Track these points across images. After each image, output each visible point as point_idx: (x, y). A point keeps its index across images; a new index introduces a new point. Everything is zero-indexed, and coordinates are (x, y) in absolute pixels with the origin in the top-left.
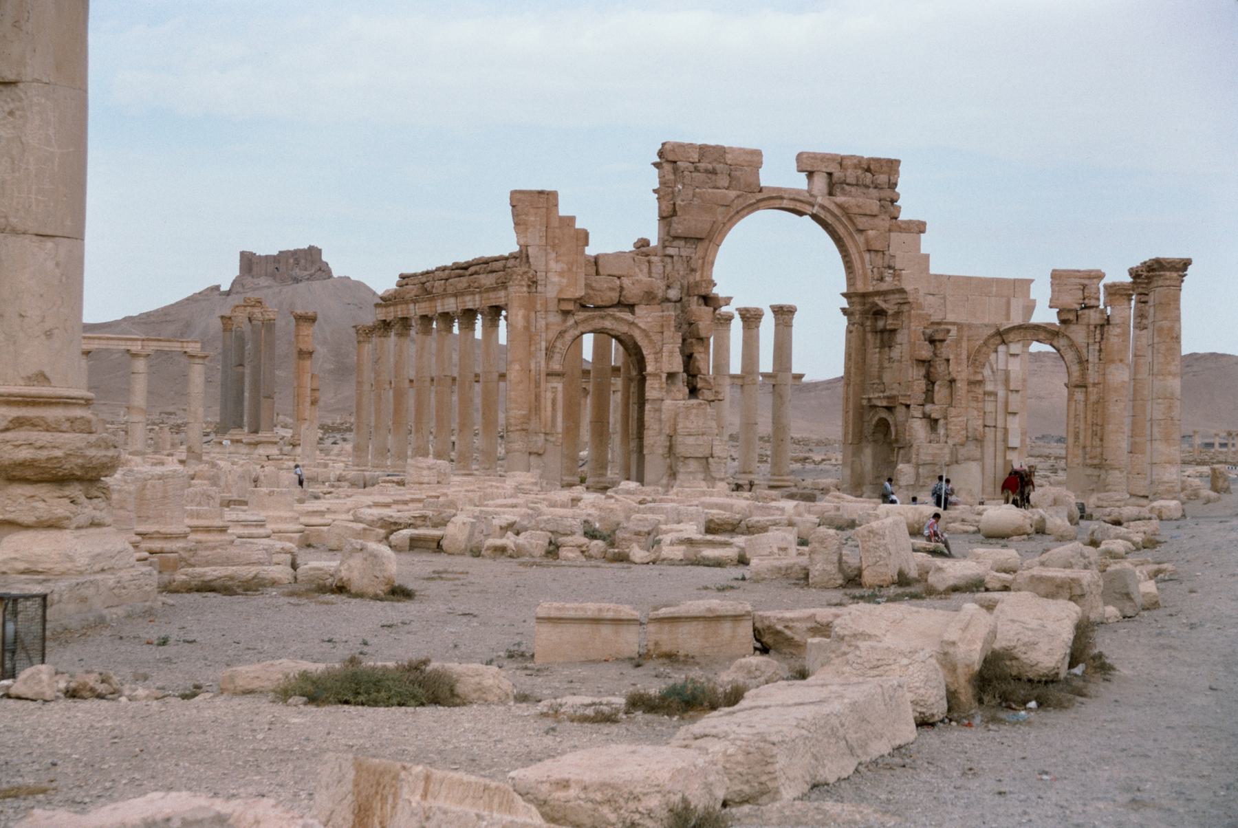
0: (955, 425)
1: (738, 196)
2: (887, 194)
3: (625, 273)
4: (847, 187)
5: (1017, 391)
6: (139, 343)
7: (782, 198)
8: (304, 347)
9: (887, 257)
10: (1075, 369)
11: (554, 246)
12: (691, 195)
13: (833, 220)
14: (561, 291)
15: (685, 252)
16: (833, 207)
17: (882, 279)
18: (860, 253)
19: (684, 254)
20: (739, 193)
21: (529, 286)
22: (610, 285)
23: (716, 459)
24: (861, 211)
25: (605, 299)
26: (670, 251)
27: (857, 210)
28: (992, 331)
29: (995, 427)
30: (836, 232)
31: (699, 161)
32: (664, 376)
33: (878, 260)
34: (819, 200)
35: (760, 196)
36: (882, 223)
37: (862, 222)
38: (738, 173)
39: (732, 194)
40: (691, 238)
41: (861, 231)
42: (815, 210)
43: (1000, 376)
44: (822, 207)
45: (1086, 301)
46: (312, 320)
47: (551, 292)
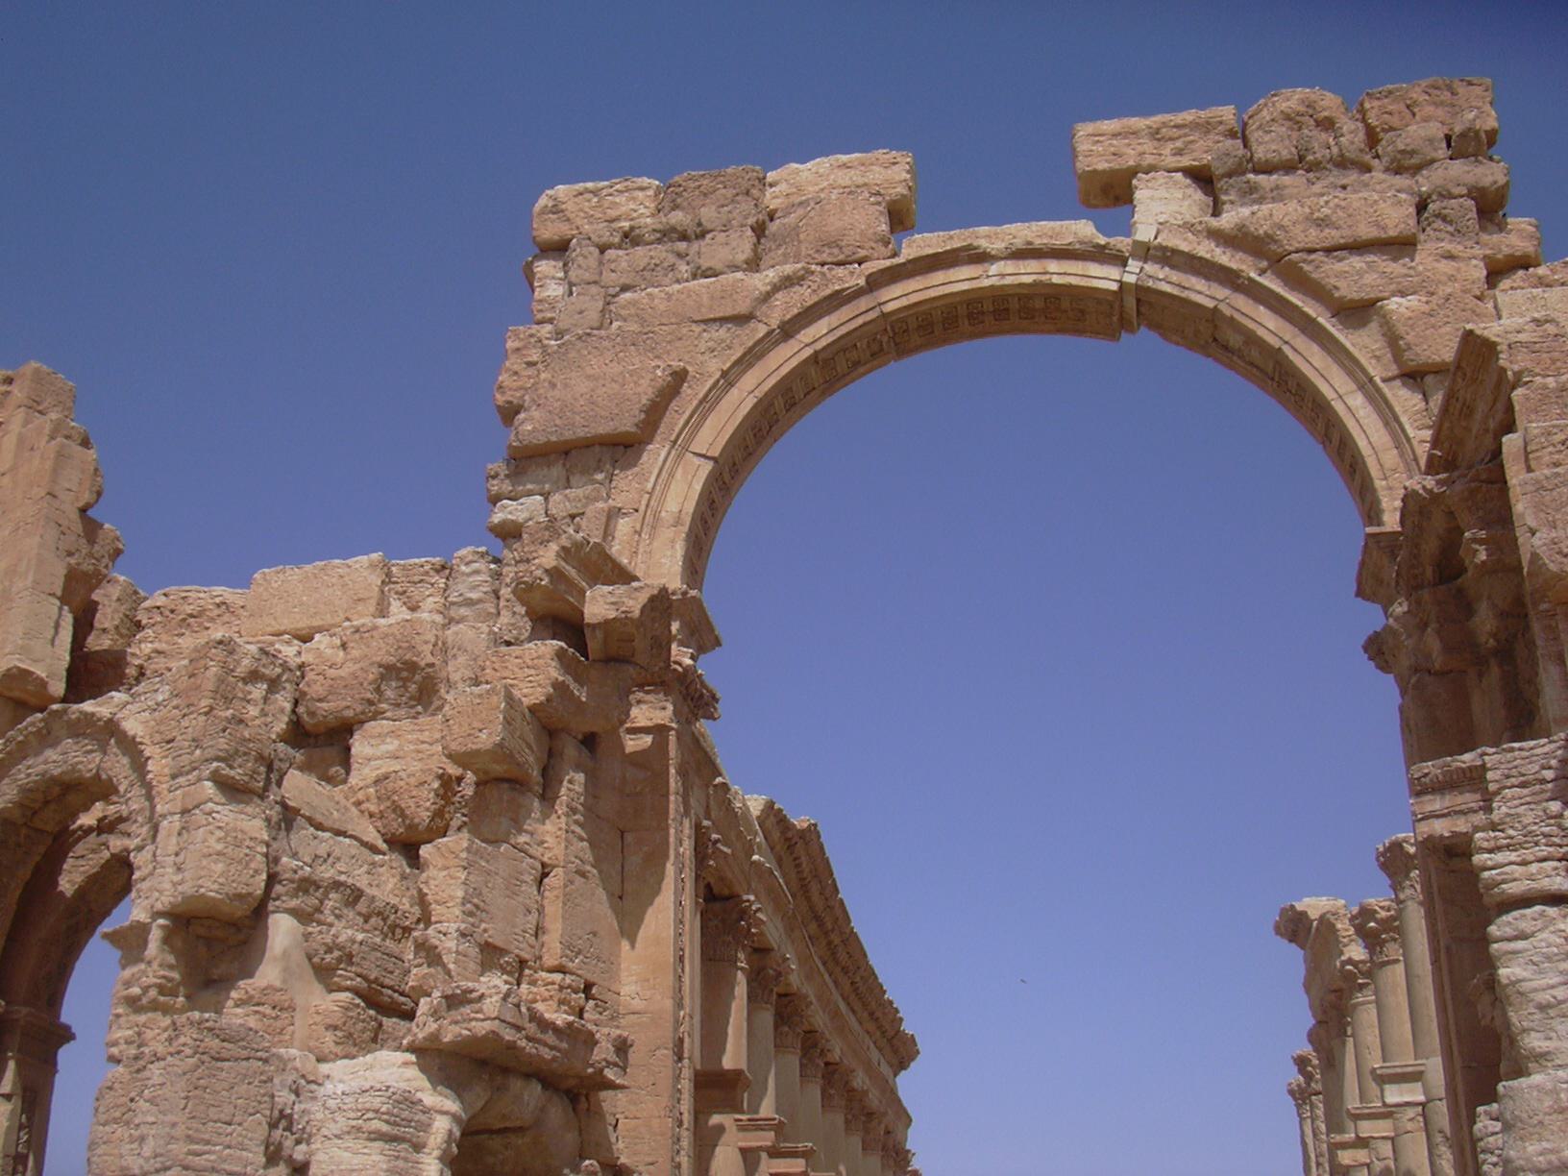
1: (788, 282)
3: (329, 620)
7: (981, 257)
12: (593, 316)
13: (1222, 292)
16: (1206, 249)
18: (1366, 385)
20: (788, 269)
24: (1333, 236)
27: (1314, 236)
37: (1352, 276)
38: (792, 219)
40: (587, 444)
41: (1358, 312)
44: (1168, 257)
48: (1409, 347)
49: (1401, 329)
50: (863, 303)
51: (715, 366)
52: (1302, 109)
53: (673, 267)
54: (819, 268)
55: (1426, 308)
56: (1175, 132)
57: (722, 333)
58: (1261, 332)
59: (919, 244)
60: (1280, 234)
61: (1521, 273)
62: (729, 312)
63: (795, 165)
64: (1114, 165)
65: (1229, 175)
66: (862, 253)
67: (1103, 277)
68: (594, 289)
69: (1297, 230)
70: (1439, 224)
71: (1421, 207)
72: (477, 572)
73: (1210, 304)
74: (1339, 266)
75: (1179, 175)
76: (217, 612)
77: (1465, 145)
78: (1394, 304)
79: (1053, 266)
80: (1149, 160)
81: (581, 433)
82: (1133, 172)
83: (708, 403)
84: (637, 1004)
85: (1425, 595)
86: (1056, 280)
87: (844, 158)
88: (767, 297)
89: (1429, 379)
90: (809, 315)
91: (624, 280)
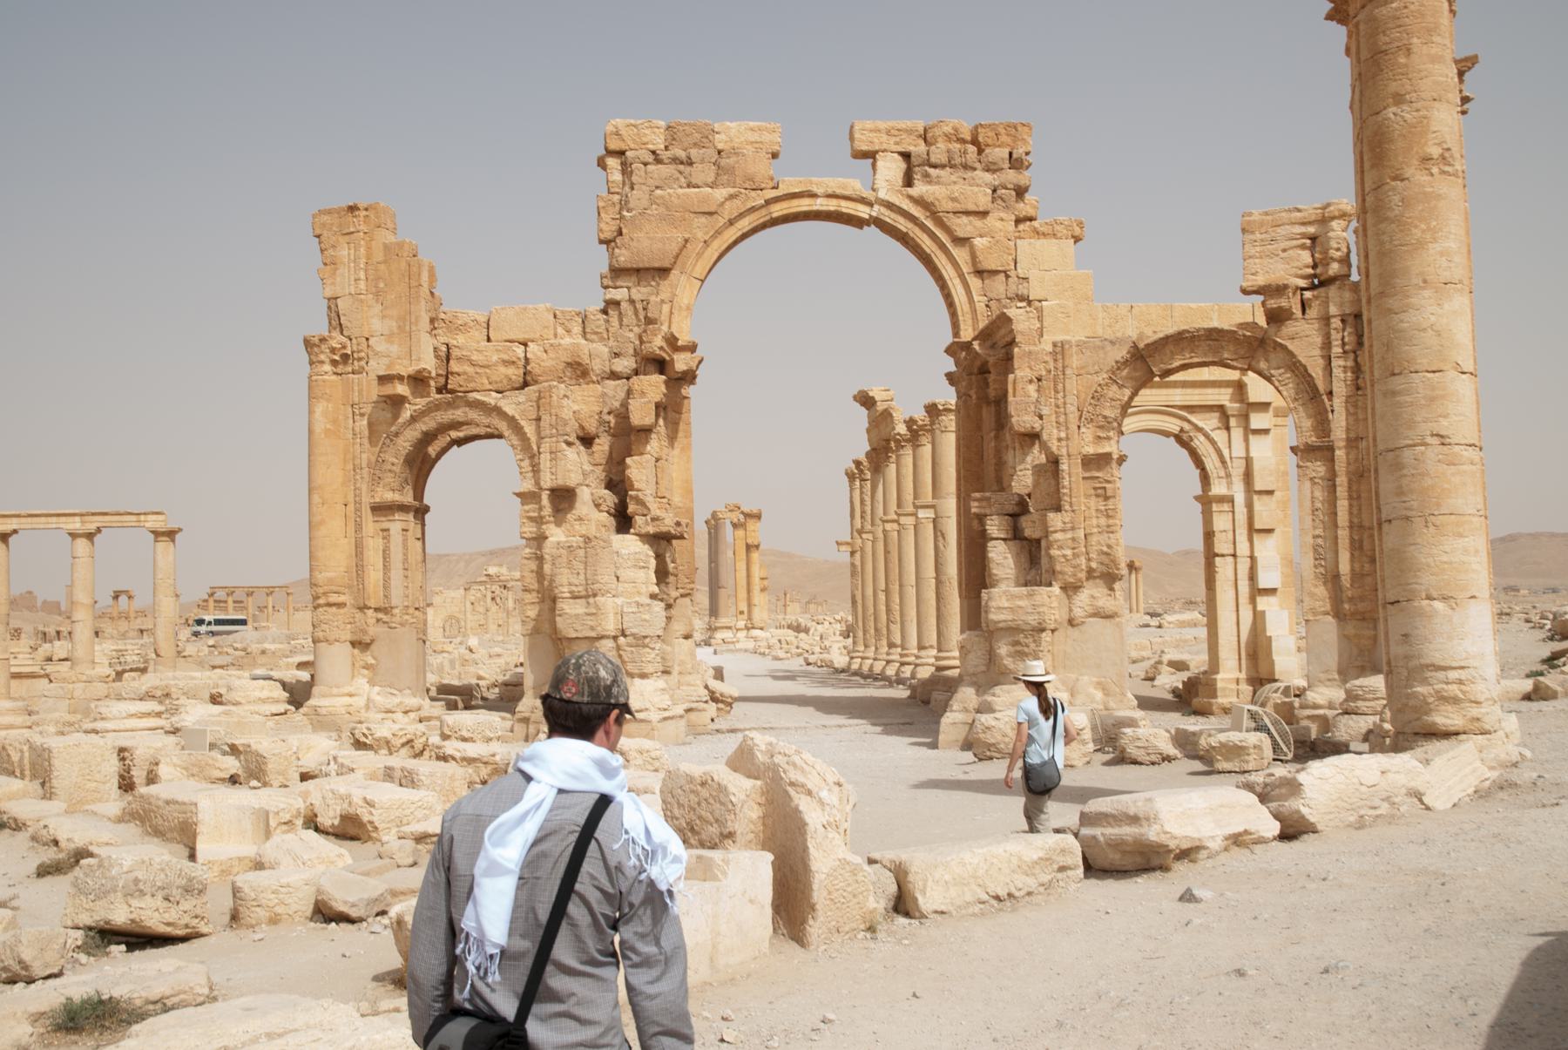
0: (1060, 548)
1: (732, 197)
2: (1011, 176)
4: (931, 171)
5: (1270, 493)
6: (77, 519)
7: (813, 195)
8: (749, 541)
9: (1013, 280)
11: (377, 294)
13: (910, 225)
14: (389, 367)
15: (638, 293)
16: (907, 205)
18: (961, 276)
19: (636, 295)
20: (732, 191)
21: (334, 363)
22: (506, 357)
23: (630, 639)
24: (958, 207)
25: (494, 378)
26: (619, 294)
27: (950, 206)
28: (1122, 353)
29: (1234, 556)
30: (918, 246)
31: (666, 148)
32: (545, 496)
33: (998, 286)
34: (882, 194)
35: (774, 194)
36: (999, 224)
37: (963, 226)
38: (732, 161)
39: (720, 193)
40: (647, 269)
41: (961, 241)
42: (877, 211)
43: (1237, 470)
44: (890, 206)
45: (1318, 271)
46: (758, 517)
47: (377, 367)
48: (980, 262)
49: (978, 253)
50: (764, 212)
51: (700, 235)
52: (952, 132)
53: (678, 179)
54: (743, 191)
55: (988, 245)
56: (896, 133)
57: (703, 219)
58: (924, 246)
60: (937, 203)
61: (1028, 223)
62: (707, 210)
63: (728, 123)
64: (870, 148)
65: (919, 166)
66: (763, 186)
67: (863, 211)
68: (644, 187)
69: (944, 202)
70: (1000, 202)
71: (994, 191)
72: (599, 320)
73: (905, 230)
74: (958, 221)
75: (896, 155)
76: (472, 324)
77: (1016, 163)
78: (978, 242)
79: (844, 203)
80: (885, 146)
81: (647, 265)
82: (877, 152)
83: (700, 255)
84: (680, 505)
85: (973, 377)
86: (844, 210)
87: (751, 124)
88: (722, 204)
89: (985, 274)
90: (741, 216)
91: (657, 184)
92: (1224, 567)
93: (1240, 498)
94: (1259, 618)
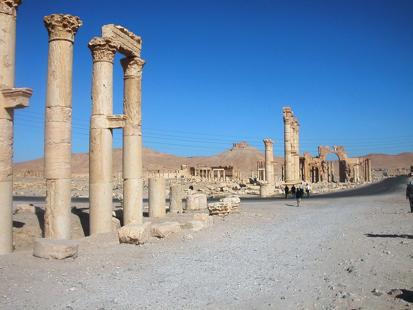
10: (363, 168)
11: (308, 158)
17: (343, 159)
37: (340, 153)
42: (335, 152)
59: (330, 150)
67: (334, 152)
92: (355, 175)
93: (356, 171)
94: (357, 178)
